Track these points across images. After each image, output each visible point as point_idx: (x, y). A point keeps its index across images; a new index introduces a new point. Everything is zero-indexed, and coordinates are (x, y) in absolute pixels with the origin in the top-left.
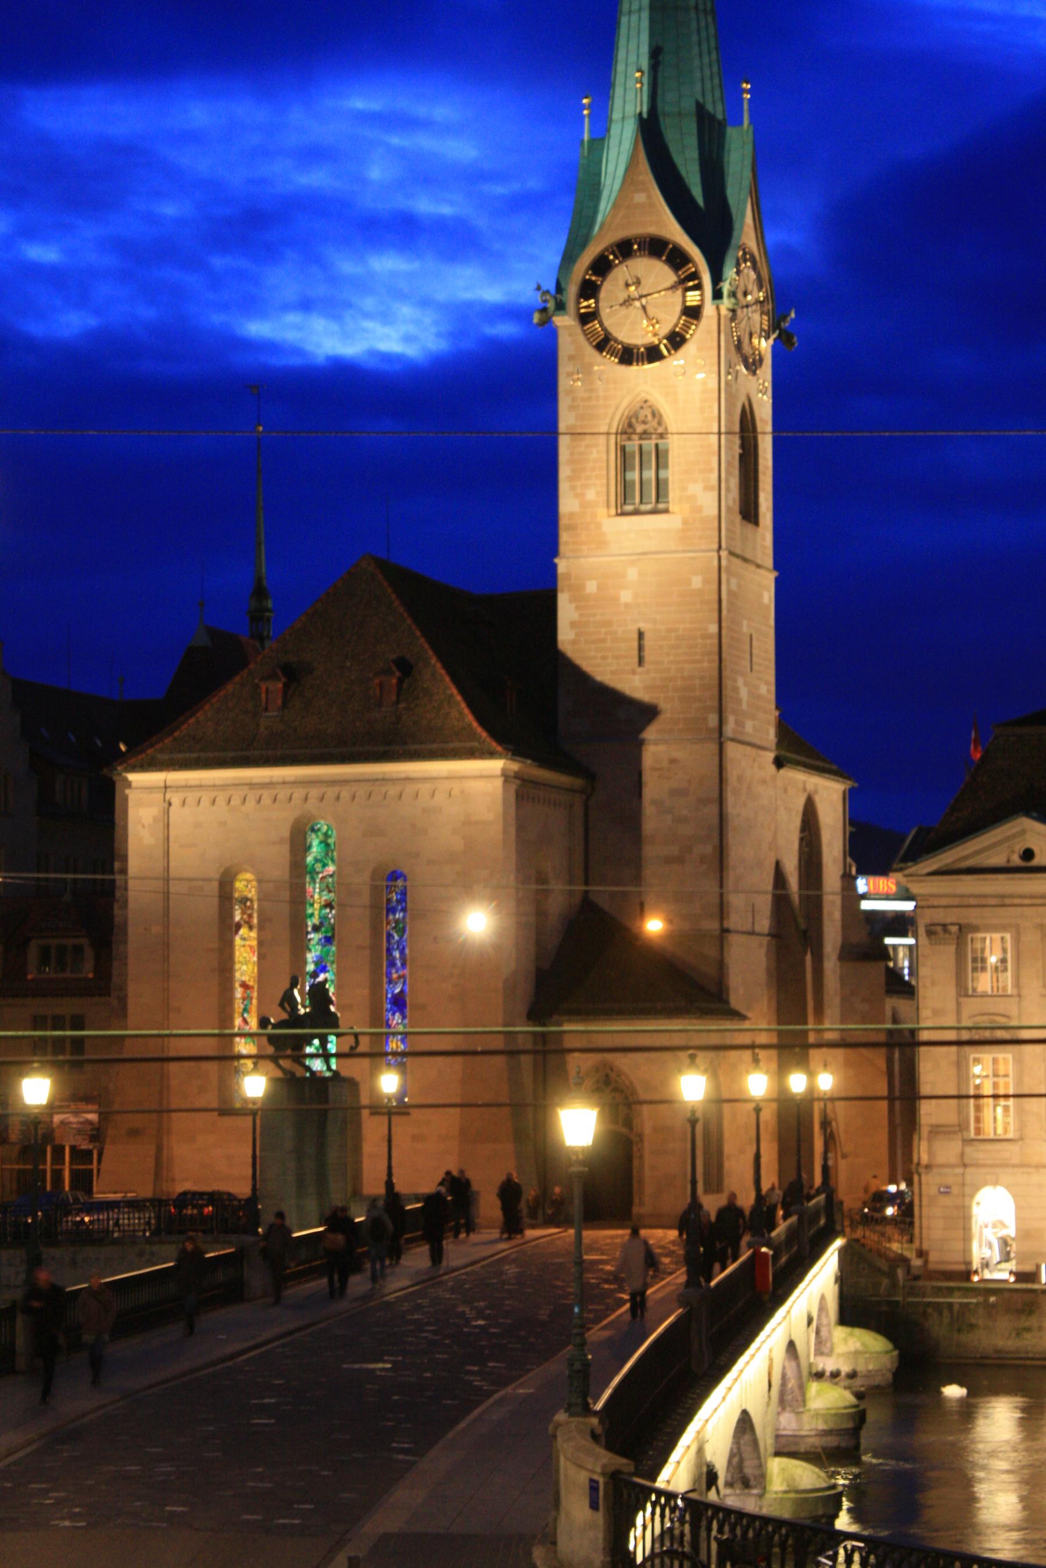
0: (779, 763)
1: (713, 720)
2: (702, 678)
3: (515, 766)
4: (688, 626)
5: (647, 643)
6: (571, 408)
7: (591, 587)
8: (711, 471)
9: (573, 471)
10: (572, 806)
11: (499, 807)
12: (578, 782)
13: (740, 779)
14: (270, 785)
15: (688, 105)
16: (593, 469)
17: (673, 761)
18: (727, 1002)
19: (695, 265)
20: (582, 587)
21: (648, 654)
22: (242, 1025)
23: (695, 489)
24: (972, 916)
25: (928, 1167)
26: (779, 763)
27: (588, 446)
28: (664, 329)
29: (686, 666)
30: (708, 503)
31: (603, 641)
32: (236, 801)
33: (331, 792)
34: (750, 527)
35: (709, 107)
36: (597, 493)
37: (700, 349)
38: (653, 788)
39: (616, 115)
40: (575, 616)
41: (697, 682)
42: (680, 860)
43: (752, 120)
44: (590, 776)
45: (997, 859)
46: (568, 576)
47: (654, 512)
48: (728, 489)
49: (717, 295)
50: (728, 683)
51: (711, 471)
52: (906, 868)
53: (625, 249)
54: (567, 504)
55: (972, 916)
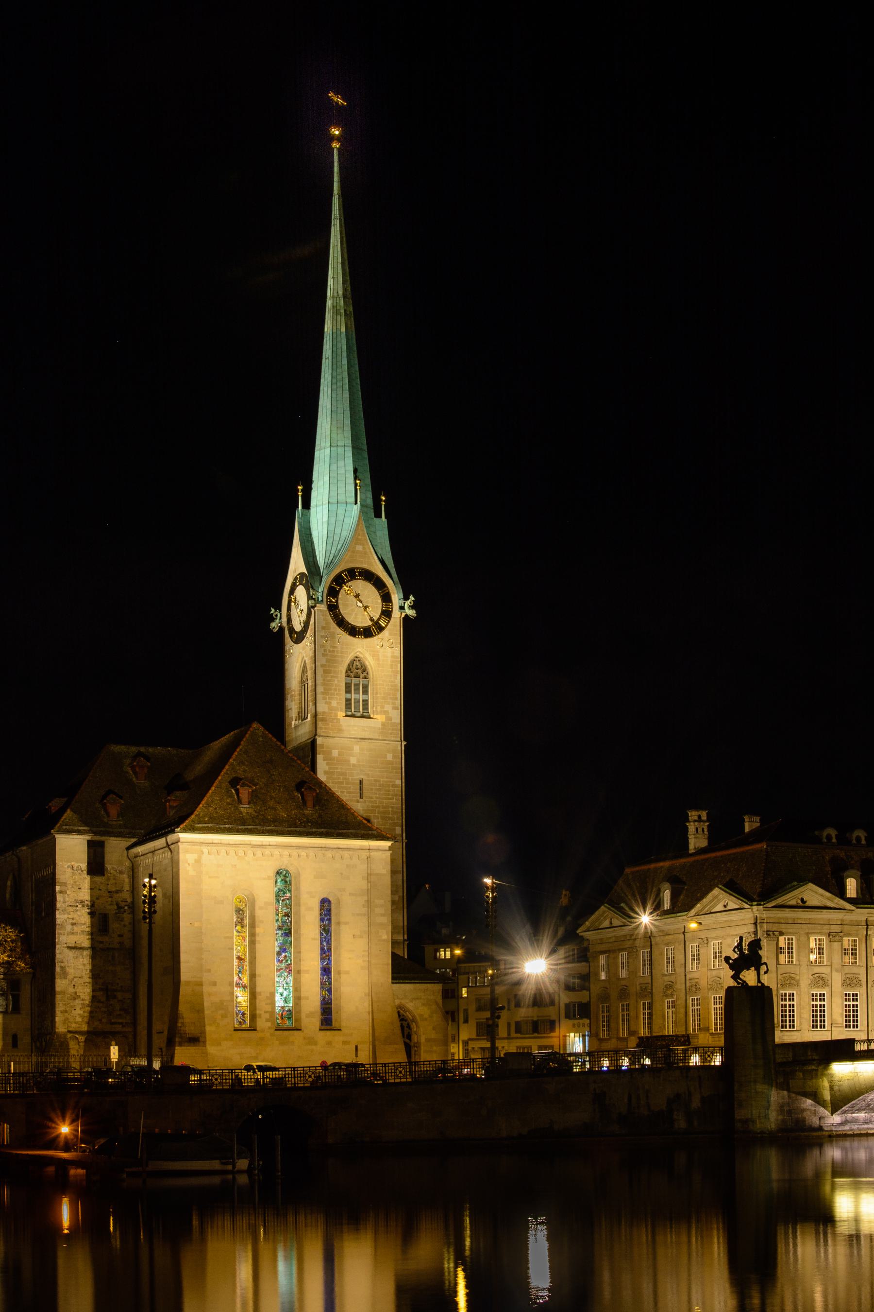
2: (392, 808)
4: (385, 779)
5: (364, 786)
6: (324, 655)
7: (335, 753)
8: (396, 699)
9: (324, 689)
14: (262, 846)
16: (335, 690)
19: (388, 588)
22: (239, 980)
23: (388, 708)
24: (783, 928)
27: (332, 677)
31: (342, 783)
32: (241, 853)
33: (295, 853)
36: (337, 703)
37: (390, 634)
40: (327, 768)
45: (793, 902)
46: (322, 746)
47: (362, 717)
51: (396, 699)
52: (764, 904)
55: (783, 928)
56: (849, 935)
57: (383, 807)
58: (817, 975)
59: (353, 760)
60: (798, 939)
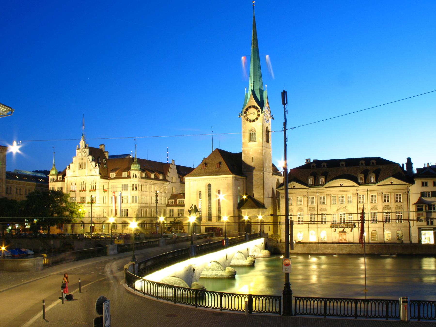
0: (273, 175)
1: (262, 169)
3: (234, 176)
5: (253, 159)
6: (243, 128)
7: (246, 152)
9: (244, 136)
10: (244, 181)
11: (232, 181)
12: (245, 178)
13: (266, 177)
15: (258, 88)
17: (257, 175)
18: (264, 207)
20: (245, 152)
21: (253, 160)
25: (281, 228)
26: (273, 175)
28: (255, 118)
29: (259, 162)
30: (261, 140)
31: (248, 159)
33: (210, 180)
34: (268, 144)
35: (261, 88)
38: (255, 178)
39: (249, 90)
41: (260, 164)
42: (258, 188)
43: (267, 90)
44: (246, 177)
47: (254, 142)
48: (264, 138)
49: (262, 113)
50: (264, 164)
53: (250, 107)
54: (243, 141)
56: (311, 196)
57: (258, 164)
58: (299, 208)
59: (251, 153)
60: (293, 198)
